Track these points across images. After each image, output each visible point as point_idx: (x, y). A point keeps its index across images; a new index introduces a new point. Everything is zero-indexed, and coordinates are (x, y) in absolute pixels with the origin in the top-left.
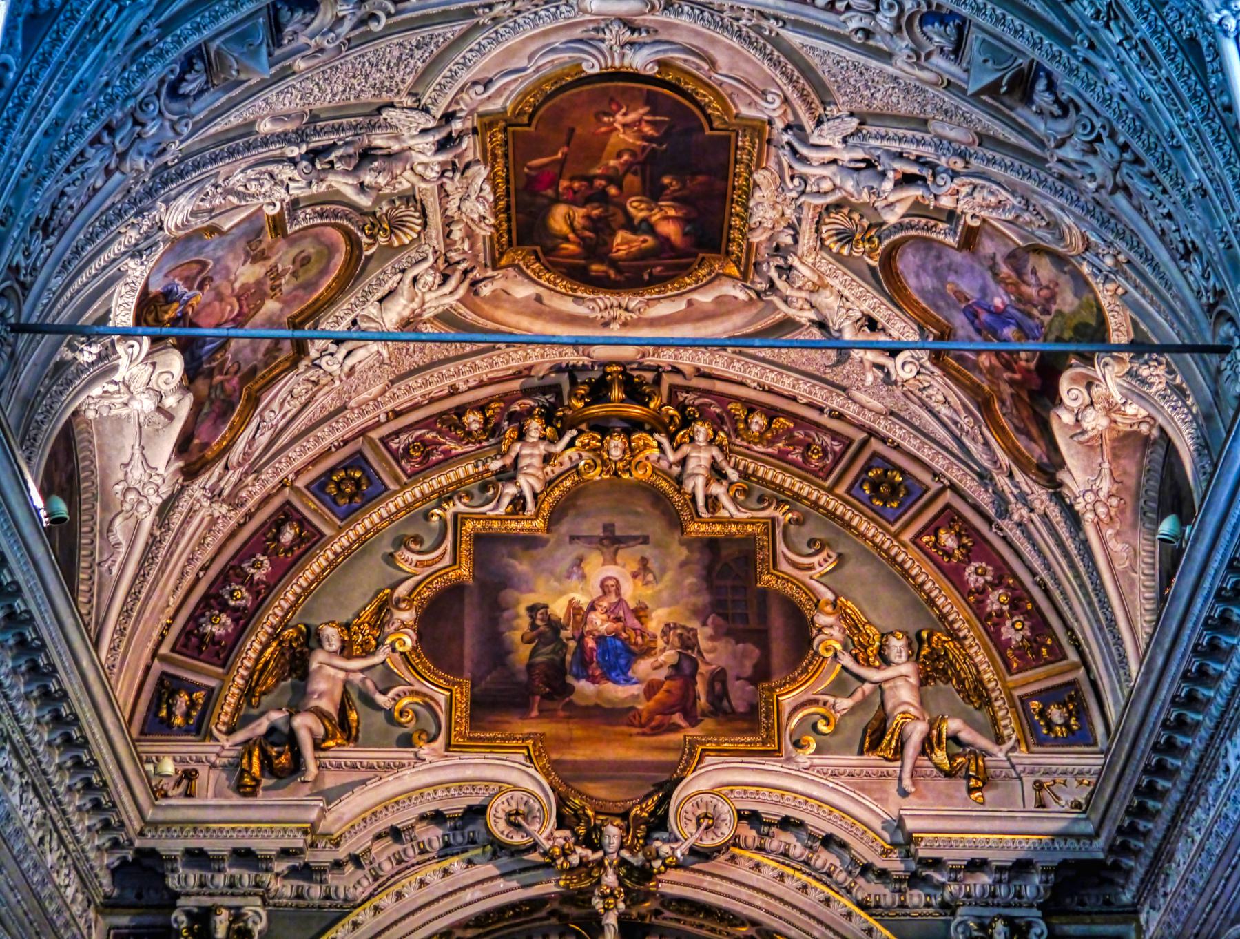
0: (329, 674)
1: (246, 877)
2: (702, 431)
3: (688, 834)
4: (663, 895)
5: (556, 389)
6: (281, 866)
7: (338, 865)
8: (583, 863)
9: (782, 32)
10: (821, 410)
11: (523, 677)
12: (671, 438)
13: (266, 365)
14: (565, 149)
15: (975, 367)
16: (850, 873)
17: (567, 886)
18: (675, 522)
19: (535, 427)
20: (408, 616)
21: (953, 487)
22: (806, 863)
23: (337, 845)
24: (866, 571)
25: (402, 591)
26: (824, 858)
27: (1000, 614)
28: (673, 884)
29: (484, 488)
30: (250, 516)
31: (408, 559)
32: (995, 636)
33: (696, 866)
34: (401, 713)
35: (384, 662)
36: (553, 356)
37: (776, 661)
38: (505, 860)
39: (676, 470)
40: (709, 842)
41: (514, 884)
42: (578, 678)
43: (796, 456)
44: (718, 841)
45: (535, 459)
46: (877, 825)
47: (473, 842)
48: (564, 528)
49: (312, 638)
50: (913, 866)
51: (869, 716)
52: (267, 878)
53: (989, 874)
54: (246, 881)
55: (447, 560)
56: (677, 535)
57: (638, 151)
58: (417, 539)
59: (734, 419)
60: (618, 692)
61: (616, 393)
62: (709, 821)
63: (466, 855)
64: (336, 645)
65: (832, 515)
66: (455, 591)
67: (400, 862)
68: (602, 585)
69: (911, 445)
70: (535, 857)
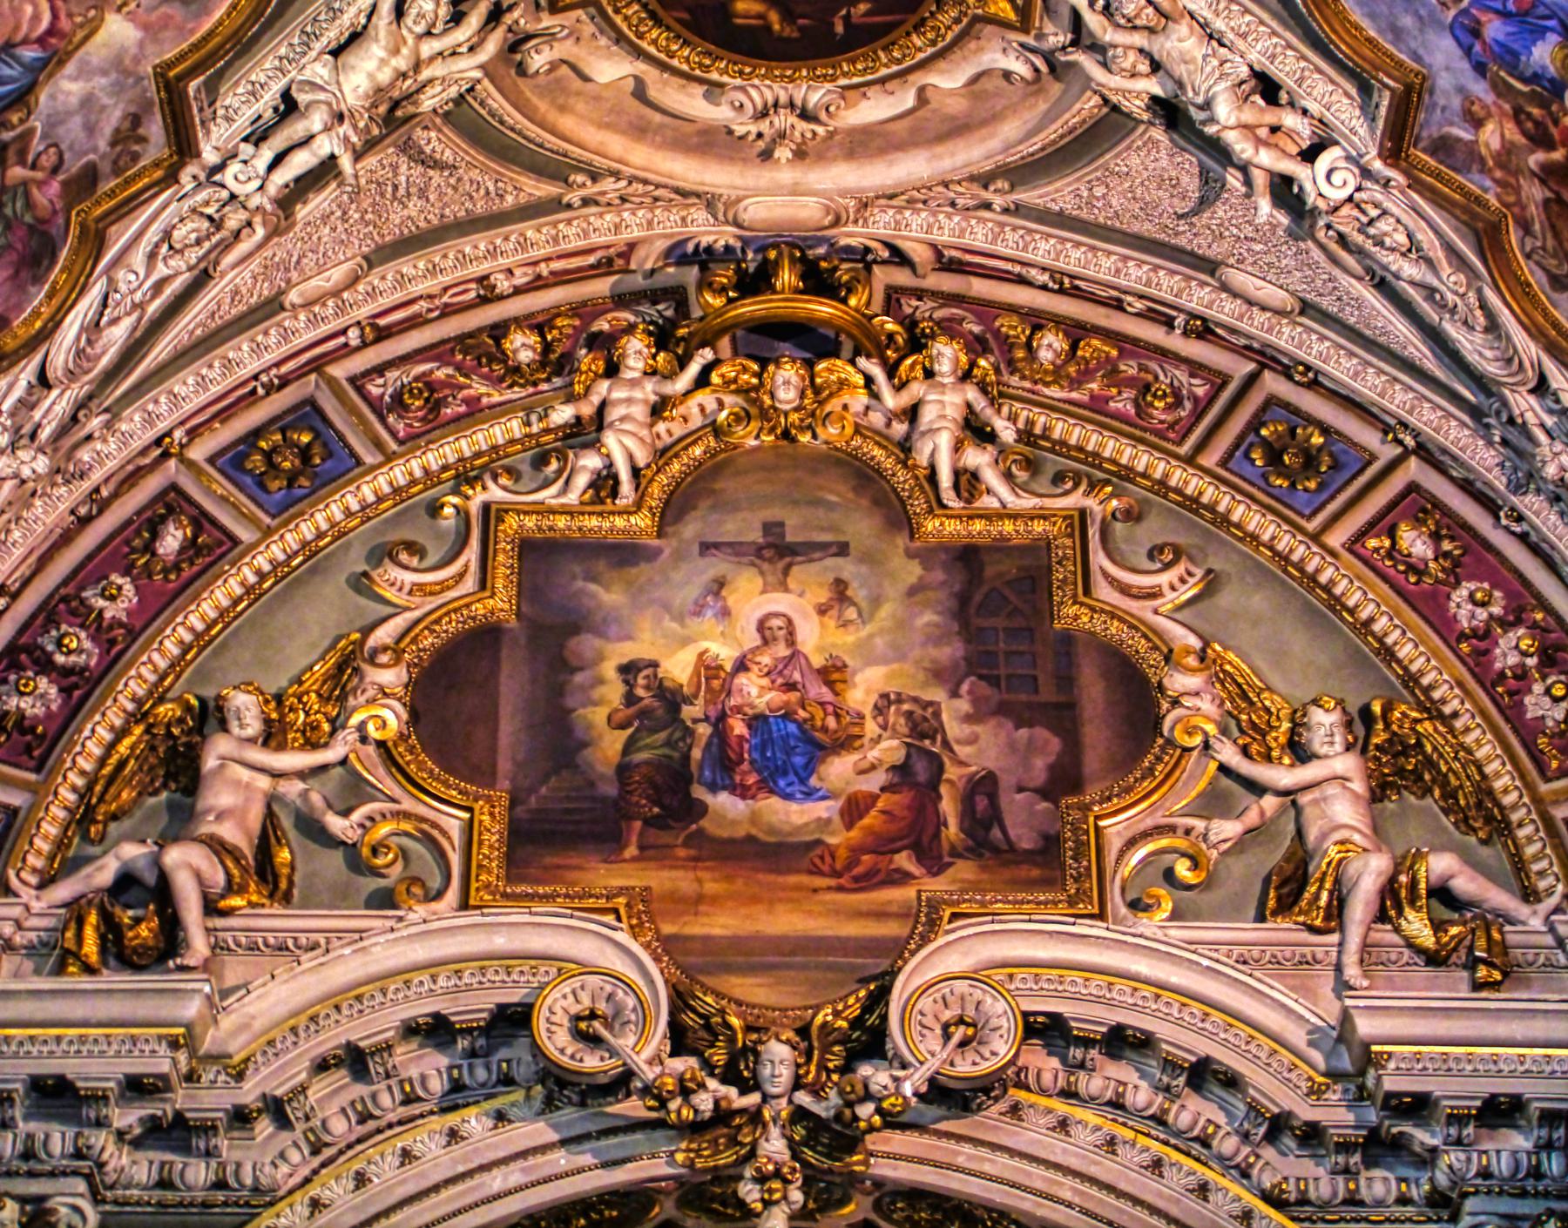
0: (240, 781)
1: (56, 1139)
2: (946, 355)
3: (924, 1054)
4: (879, 1183)
5: (677, 296)
6: (128, 1117)
7: (241, 1118)
8: (722, 1115)
10: (1169, 323)
11: (610, 790)
12: (891, 370)
13: (117, 171)
15: (1471, 158)
16: (1246, 1137)
17: (690, 1165)
18: (899, 519)
19: (636, 352)
20: (391, 677)
21: (1423, 451)
22: (1159, 1120)
23: (240, 1076)
24: (1260, 601)
25: (383, 635)
26: (1194, 1110)
27: (1522, 674)
28: (896, 1159)
29: (541, 461)
30: (99, 503)
31: (396, 579)
32: (1513, 712)
33: (943, 1126)
34: (374, 852)
35: (344, 762)
36: (669, 224)
37: (1092, 761)
38: (568, 1114)
39: (900, 429)
40: (966, 1067)
41: (587, 1159)
42: (714, 788)
43: (1123, 403)
44: (986, 1067)
45: (637, 411)
46: (1297, 1036)
47: (507, 1081)
48: (691, 529)
49: (210, 716)
50: (1372, 1116)
51: (1272, 857)
52: (100, 1140)
53: (1526, 1132)
54: (56, 1147)
55: (470, 584)
56: (901, 541)
58: (412, 548)
59: (1007, 345)
60: (790, 814)
61: (787, 277)
62: (967, 1031)
63: (496, 1103)
64: (254, 727)
65: (1193, 504)
66: (486, 636)
67: (364, 1118)
68: (762, 626)
69: (1342, 367)
70: (633, 1107)
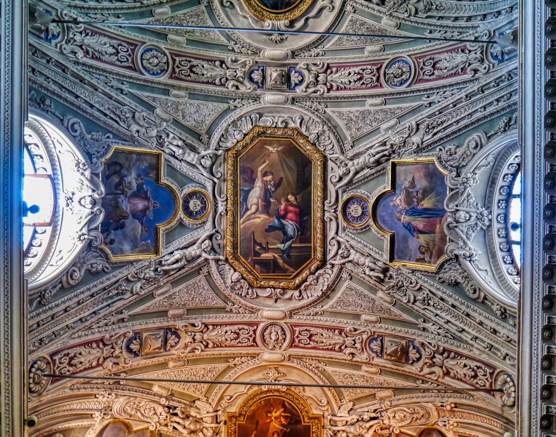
9: (326, 368)
14: (255, 432)
57: (279, 431)
